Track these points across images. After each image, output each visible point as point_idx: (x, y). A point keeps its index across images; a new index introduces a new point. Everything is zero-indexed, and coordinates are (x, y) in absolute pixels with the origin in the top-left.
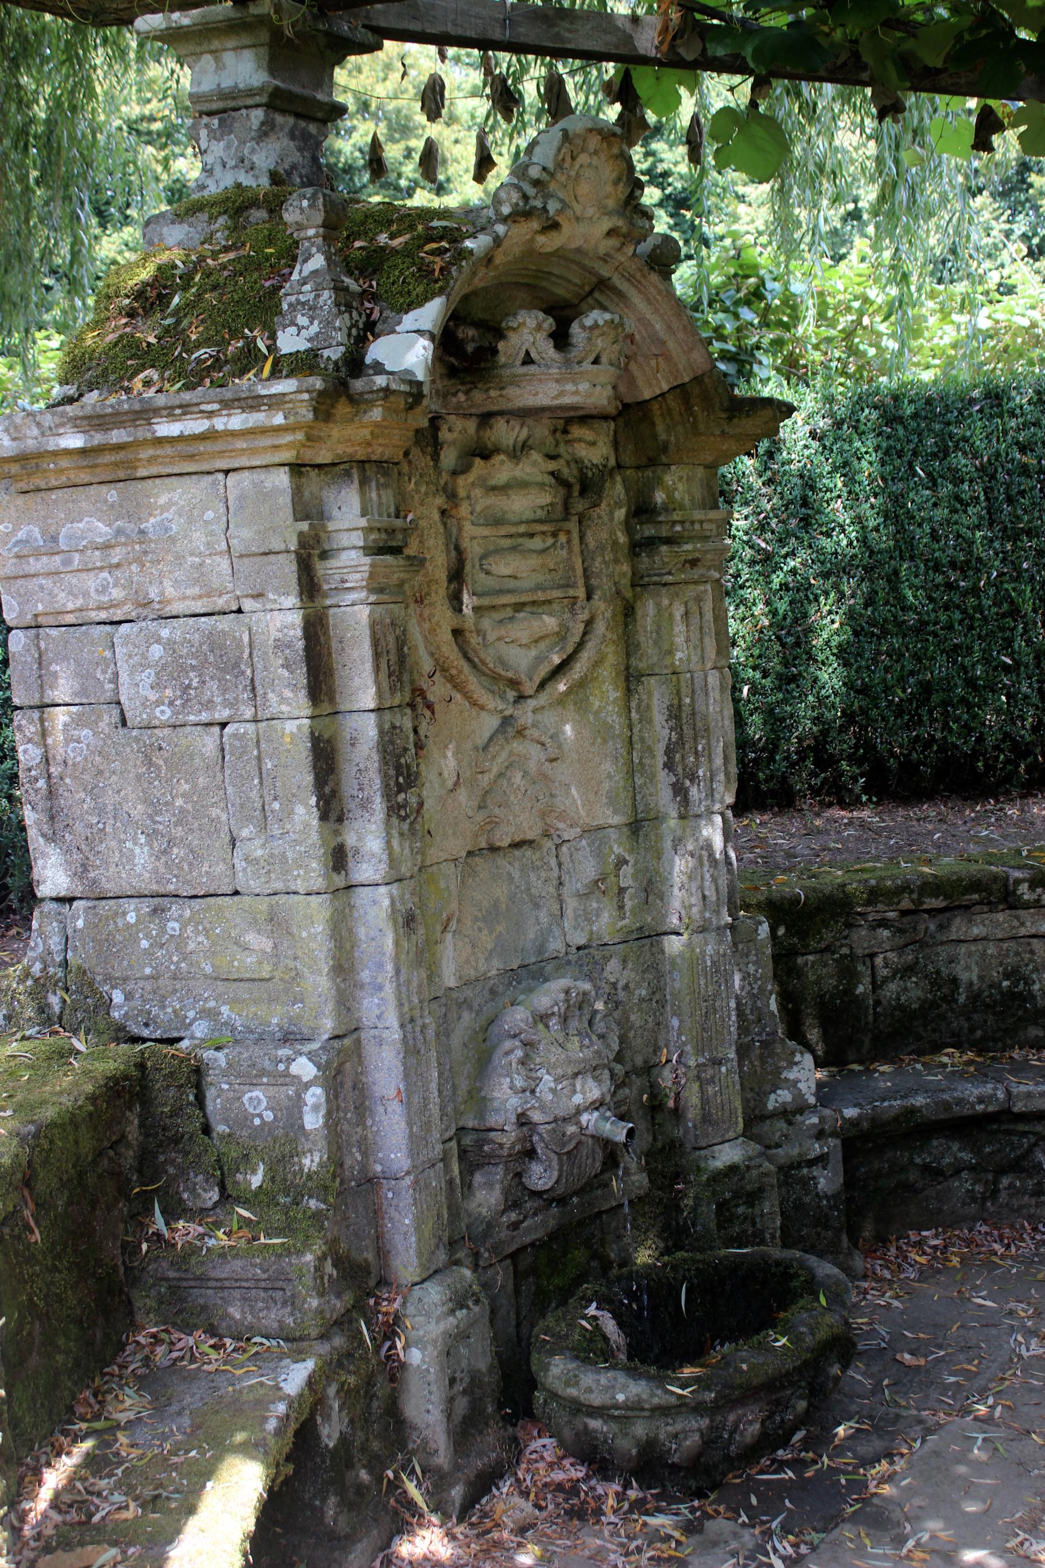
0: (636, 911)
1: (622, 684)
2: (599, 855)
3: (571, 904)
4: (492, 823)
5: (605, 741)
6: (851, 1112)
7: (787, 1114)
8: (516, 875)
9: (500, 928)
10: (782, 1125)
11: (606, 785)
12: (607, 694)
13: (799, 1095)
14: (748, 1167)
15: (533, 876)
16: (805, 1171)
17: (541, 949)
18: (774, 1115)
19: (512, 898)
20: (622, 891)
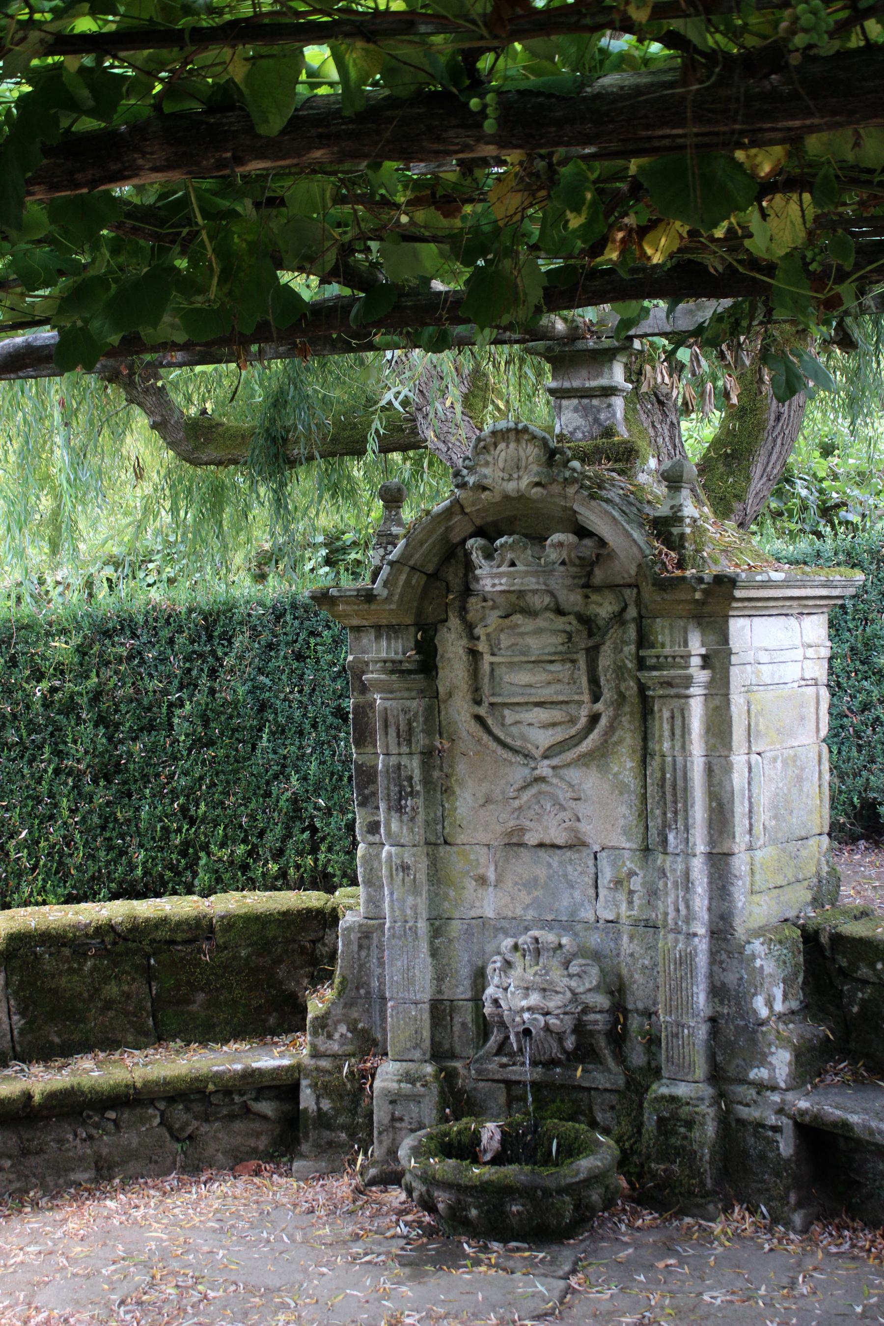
0: (641, 907)
1: (638, 756)
2: (613, 864)
3: (602, 892)
4: (522, 830)
5: (621, 793)
6: (803, 1104)
7: (762, 1087)
8: (555, 865)
9: (536, 893)
10: (753, 1092)
11: (622, 822)
12: (624, 765)
13: (773, 1078)
14: (688, 1104)
15: (570, 869)
16: (770, 1133)
17: (573, 913)
18: (752, 1083)
19: (550, 878)
20: (631, 892)
